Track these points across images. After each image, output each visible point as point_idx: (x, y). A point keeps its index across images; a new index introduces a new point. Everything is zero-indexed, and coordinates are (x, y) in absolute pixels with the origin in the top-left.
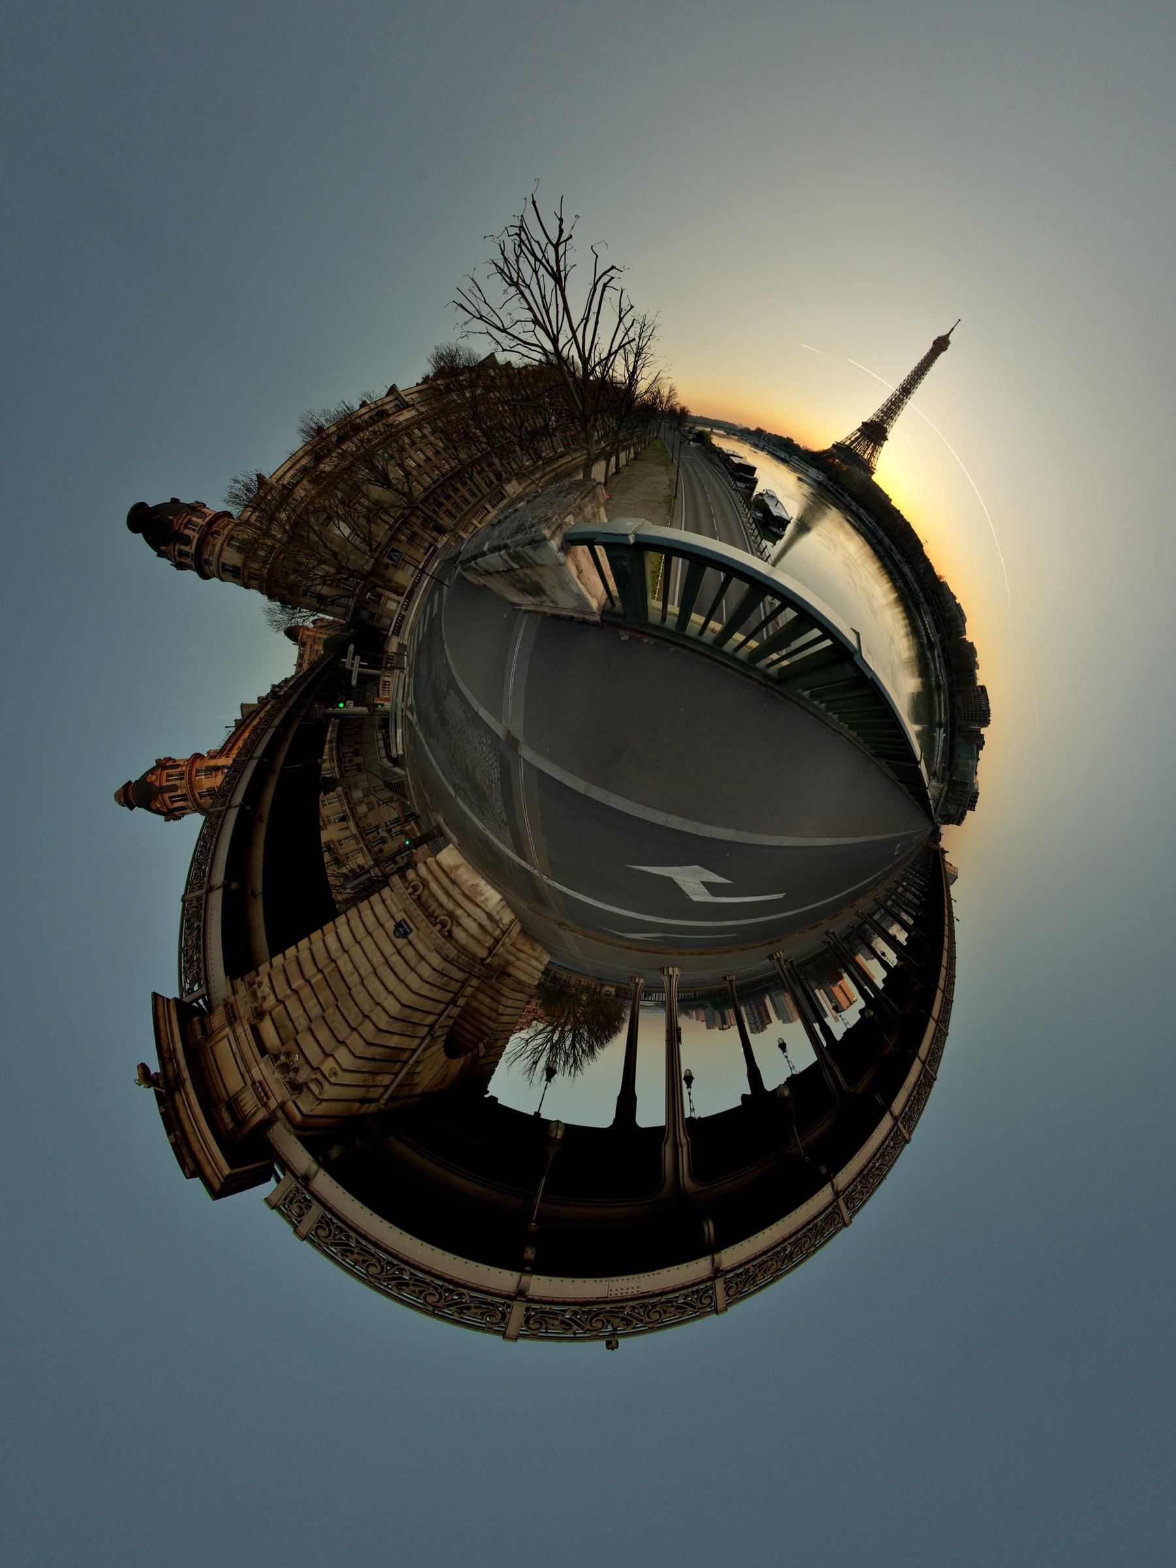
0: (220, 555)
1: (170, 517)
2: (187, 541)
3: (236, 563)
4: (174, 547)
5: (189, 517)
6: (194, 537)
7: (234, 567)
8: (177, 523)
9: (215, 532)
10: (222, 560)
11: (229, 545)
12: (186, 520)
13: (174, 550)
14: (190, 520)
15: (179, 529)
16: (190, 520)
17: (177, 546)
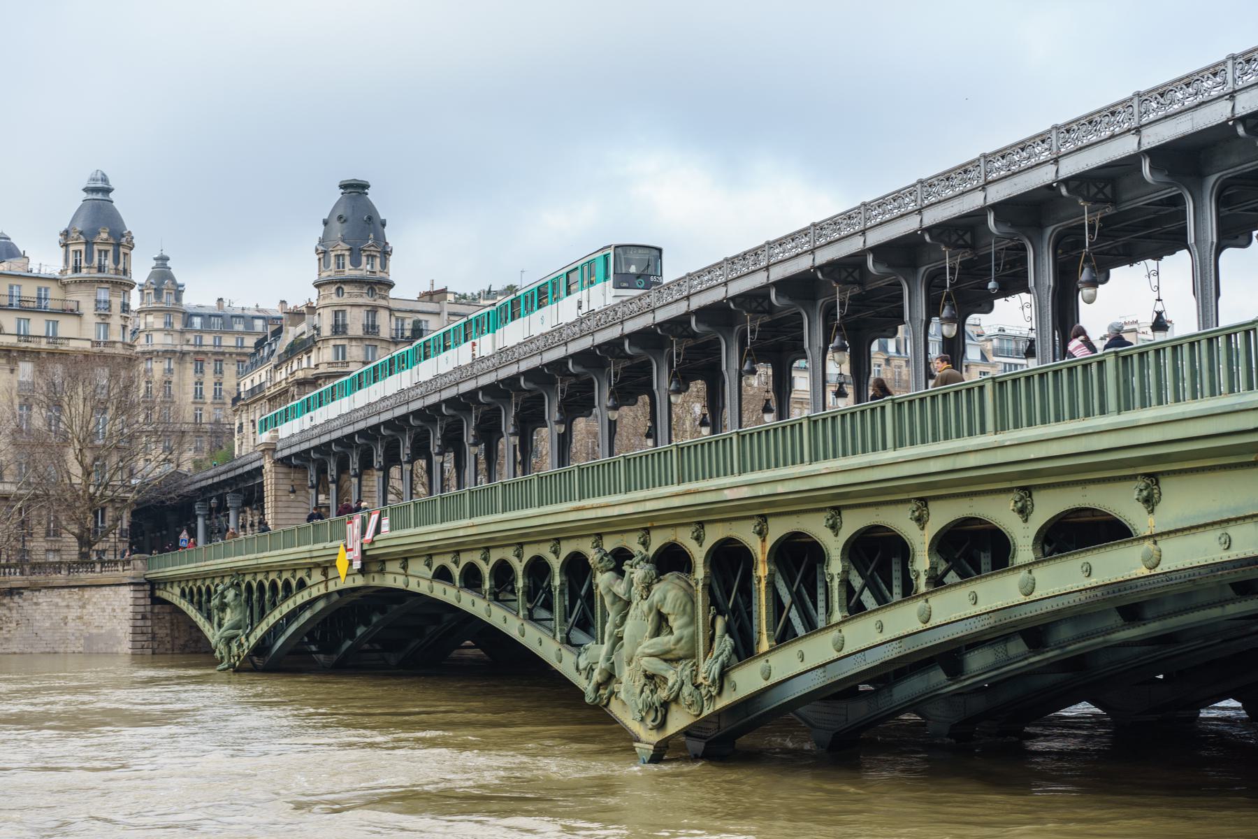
0: (352, 305)
1: (372, 236)
2: (356, 263)
3: (349, 327)
4: (346, 250)
5: (378, 255)
6: (362, 270)
7: (345, 326)
8: (370, 246)
9: (372, 289)
10: (348, 309)
11: (368, 311)
12: (375, 254)
13: (342, 250)
14: (375, 256)
15: (365, 251)
16: (375, 256)
17: (347, 253)
